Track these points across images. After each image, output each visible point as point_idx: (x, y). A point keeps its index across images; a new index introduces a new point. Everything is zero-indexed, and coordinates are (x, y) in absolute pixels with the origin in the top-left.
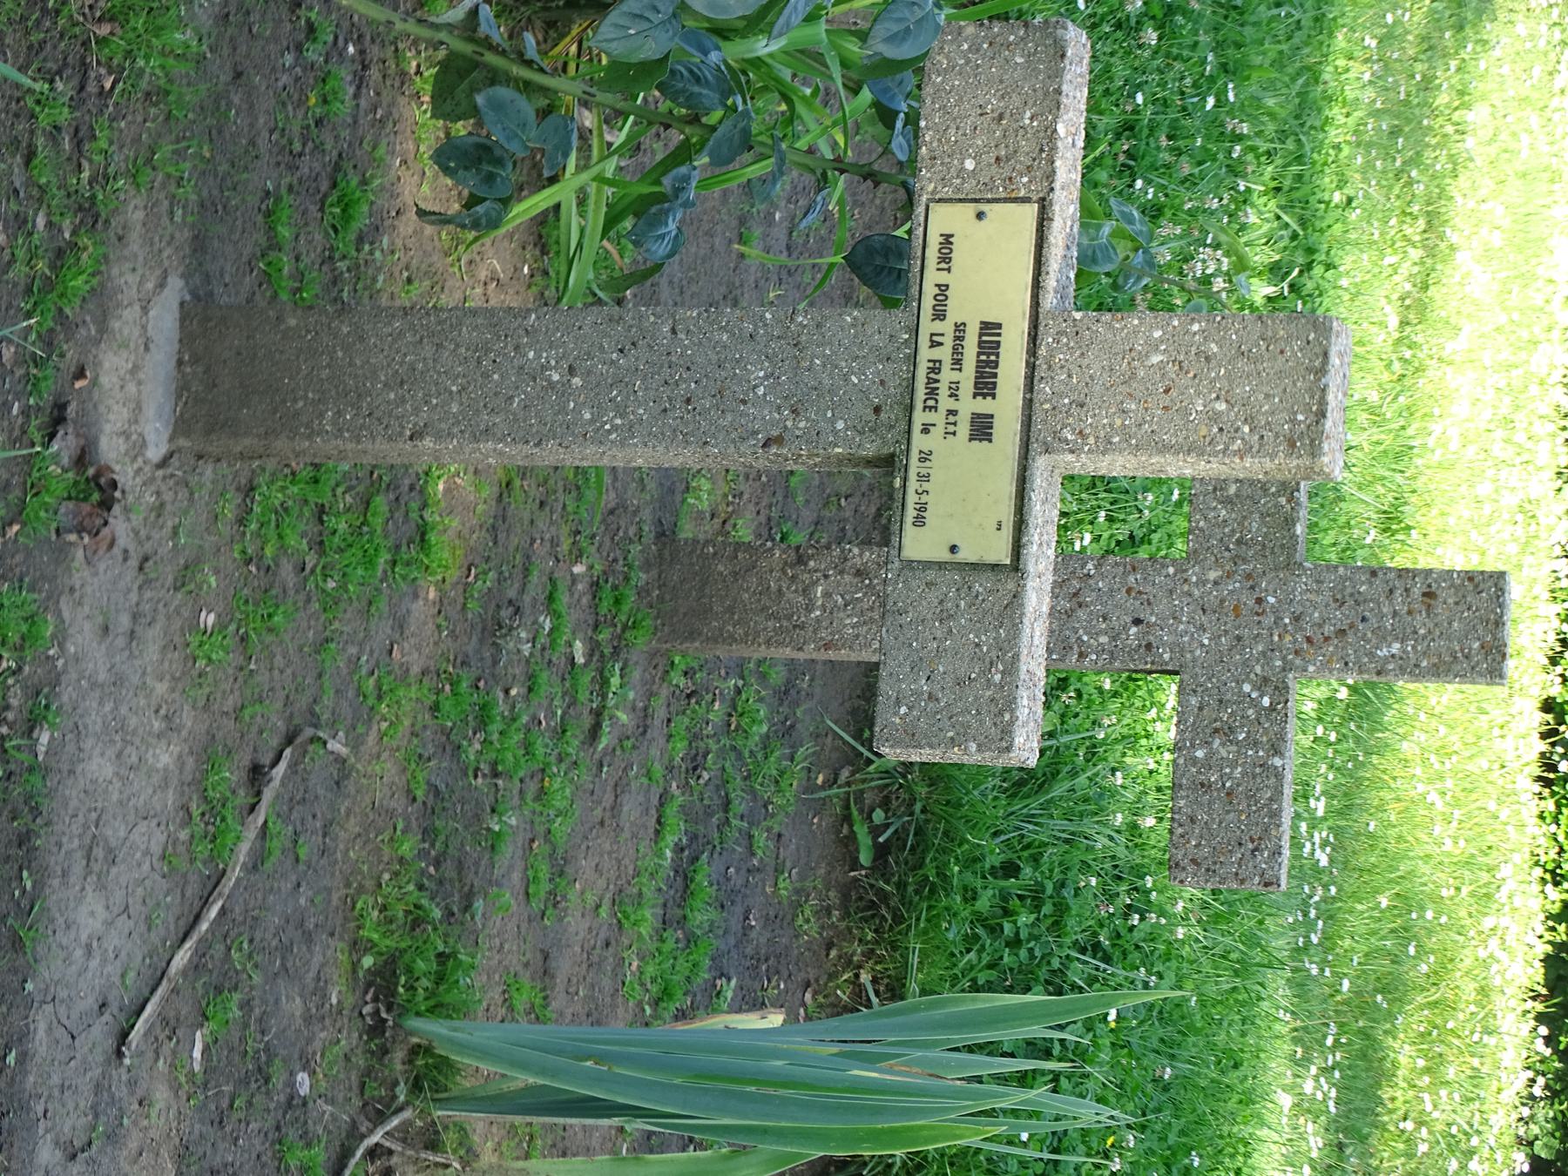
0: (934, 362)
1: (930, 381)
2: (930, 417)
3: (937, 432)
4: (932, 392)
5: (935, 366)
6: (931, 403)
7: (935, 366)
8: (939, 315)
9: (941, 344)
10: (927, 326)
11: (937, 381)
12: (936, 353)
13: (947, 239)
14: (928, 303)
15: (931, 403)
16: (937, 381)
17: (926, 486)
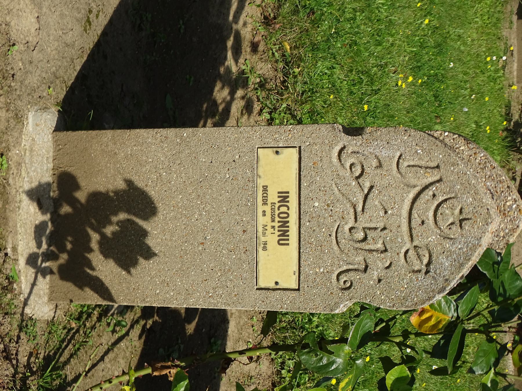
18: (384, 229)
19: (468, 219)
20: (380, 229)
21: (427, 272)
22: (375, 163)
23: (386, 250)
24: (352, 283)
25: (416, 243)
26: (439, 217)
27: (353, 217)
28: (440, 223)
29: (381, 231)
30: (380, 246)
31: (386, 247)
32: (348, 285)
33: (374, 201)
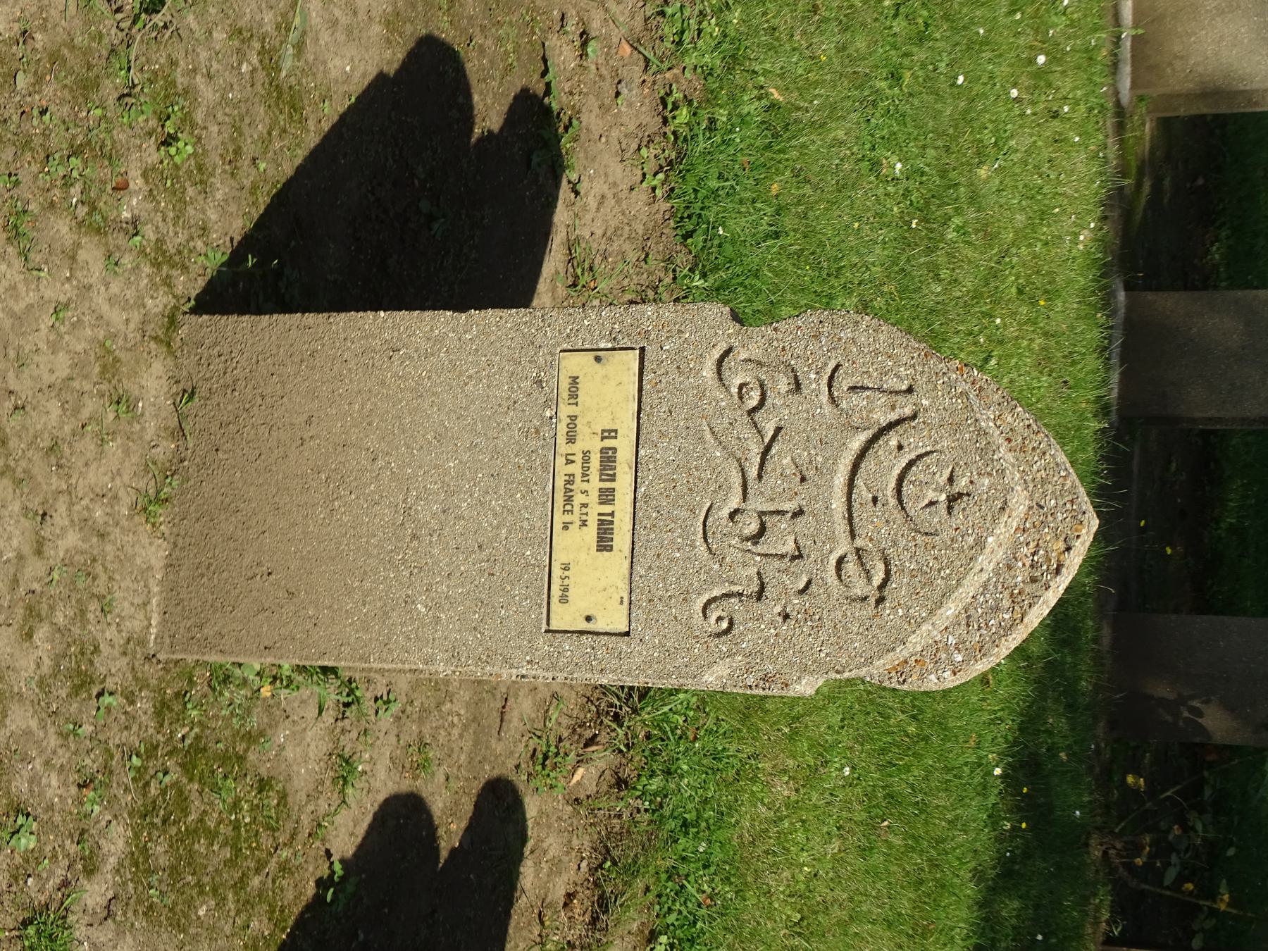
0: (570, 475)
1: (567, 490)
2: (567, 518)
3: (574, 528)
4: (569, 500)
5: (570, 480)
6: (568, 507)
7: (570, 480)
8: (571, 440)
9: (573, 462)
10: (563, 448)
11: (571, 490)
12: (571, 469)
13: (574, 380)
14: (562, 429)
15: (568, 507)
16: (571, 490)
17: (567, 573)
18: (799, 513)
19: (960, 495)
20: (790, 514)
21: (880, 600)
22: (783, 385)
23: (800, 556)
24: (731, 623)
25: (859, 542)
26: (908, 489)
27: (738, 490)
28: (909, 505)
29: (792, 517)
30: (789, 547)
31: (798, 548)
32: (725, 625)
33: (782, 458)
